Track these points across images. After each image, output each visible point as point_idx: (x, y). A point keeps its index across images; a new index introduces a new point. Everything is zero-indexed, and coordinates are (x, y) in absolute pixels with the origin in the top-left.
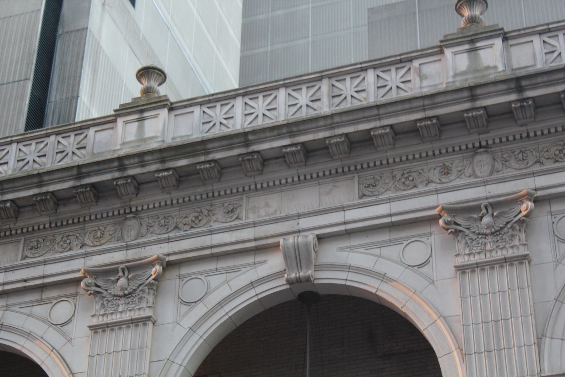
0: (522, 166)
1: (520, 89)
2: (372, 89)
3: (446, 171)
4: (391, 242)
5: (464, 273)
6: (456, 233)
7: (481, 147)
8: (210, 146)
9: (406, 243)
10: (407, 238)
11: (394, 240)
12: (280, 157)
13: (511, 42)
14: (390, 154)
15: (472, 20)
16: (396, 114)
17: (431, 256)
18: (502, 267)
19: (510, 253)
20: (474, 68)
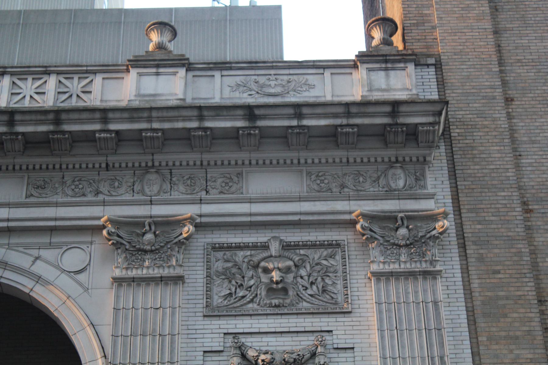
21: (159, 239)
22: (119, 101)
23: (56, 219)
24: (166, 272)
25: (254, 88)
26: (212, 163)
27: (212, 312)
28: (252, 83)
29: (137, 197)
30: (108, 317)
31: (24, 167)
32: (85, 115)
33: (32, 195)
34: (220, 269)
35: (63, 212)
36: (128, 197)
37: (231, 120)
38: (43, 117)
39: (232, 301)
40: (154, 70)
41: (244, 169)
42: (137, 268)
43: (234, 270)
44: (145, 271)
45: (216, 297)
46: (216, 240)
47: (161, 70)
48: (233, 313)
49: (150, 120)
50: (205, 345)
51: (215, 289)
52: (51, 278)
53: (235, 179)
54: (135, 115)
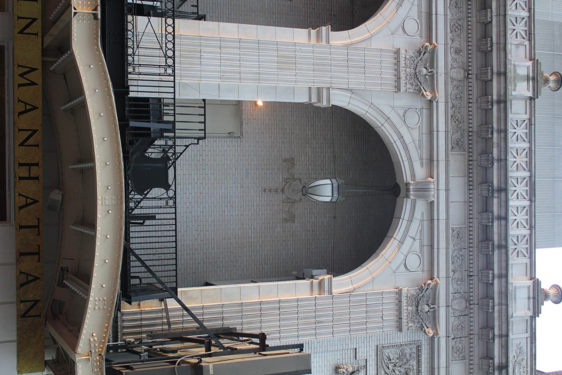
0: (452, 97)
1: (499, 102)
2: (516, 13)
3: (458, 51)
4: (420, 12)
5: (395, 53)
6: (419, 52)
7: (468, 74)
9: (418, 21)
10: (421, 22)
11: (421, 14)
13: (528, 102)
14: (474, 19)
15: (547, 81)
16: (498, 26)
17: (408, 35)
18: (395, 76)
19: (403, 81)
20: (517, 77)
21: (425, 315)
22: (512, 275)
23: (438, 249)
24: (404, 321)
25: (518, 359)
26: (471, 341)
27: (379, 350)
28: (522, 357)
29: (451, 296)
30: (378, 288)
31: (471, 225)
32: (504, 264)
33: (453, 231)
34: (406, 351)
35: (443, 252)
36: (451, 290)
37: (499, 354)
38: (503, 238)
39: (386, 361)
40: (531, 296)
41: (467, 360)
42: (407, 303)
43: (405, 360)
44: (405, 308)
45: (388, 351)
46: (423, 347)
47: (531, 300)
48: (379, 363)
49: (500, 304)
50: (360, 349)
51: (393, 350)
52: (402, 250)
53: (461, 355)
54: (503, 295)
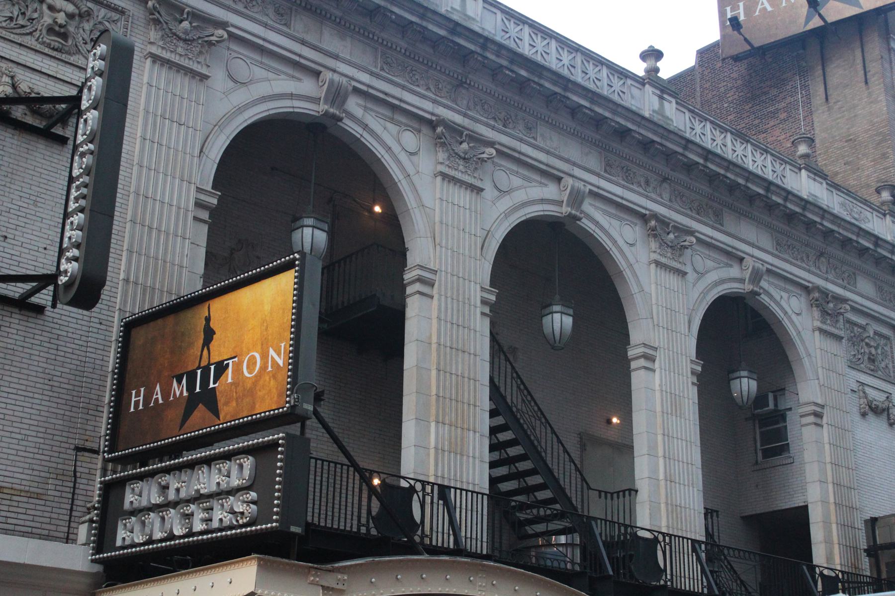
8: (545, 73)
12: (574, 111)
20: (661, 112)
47: (817, 178)
